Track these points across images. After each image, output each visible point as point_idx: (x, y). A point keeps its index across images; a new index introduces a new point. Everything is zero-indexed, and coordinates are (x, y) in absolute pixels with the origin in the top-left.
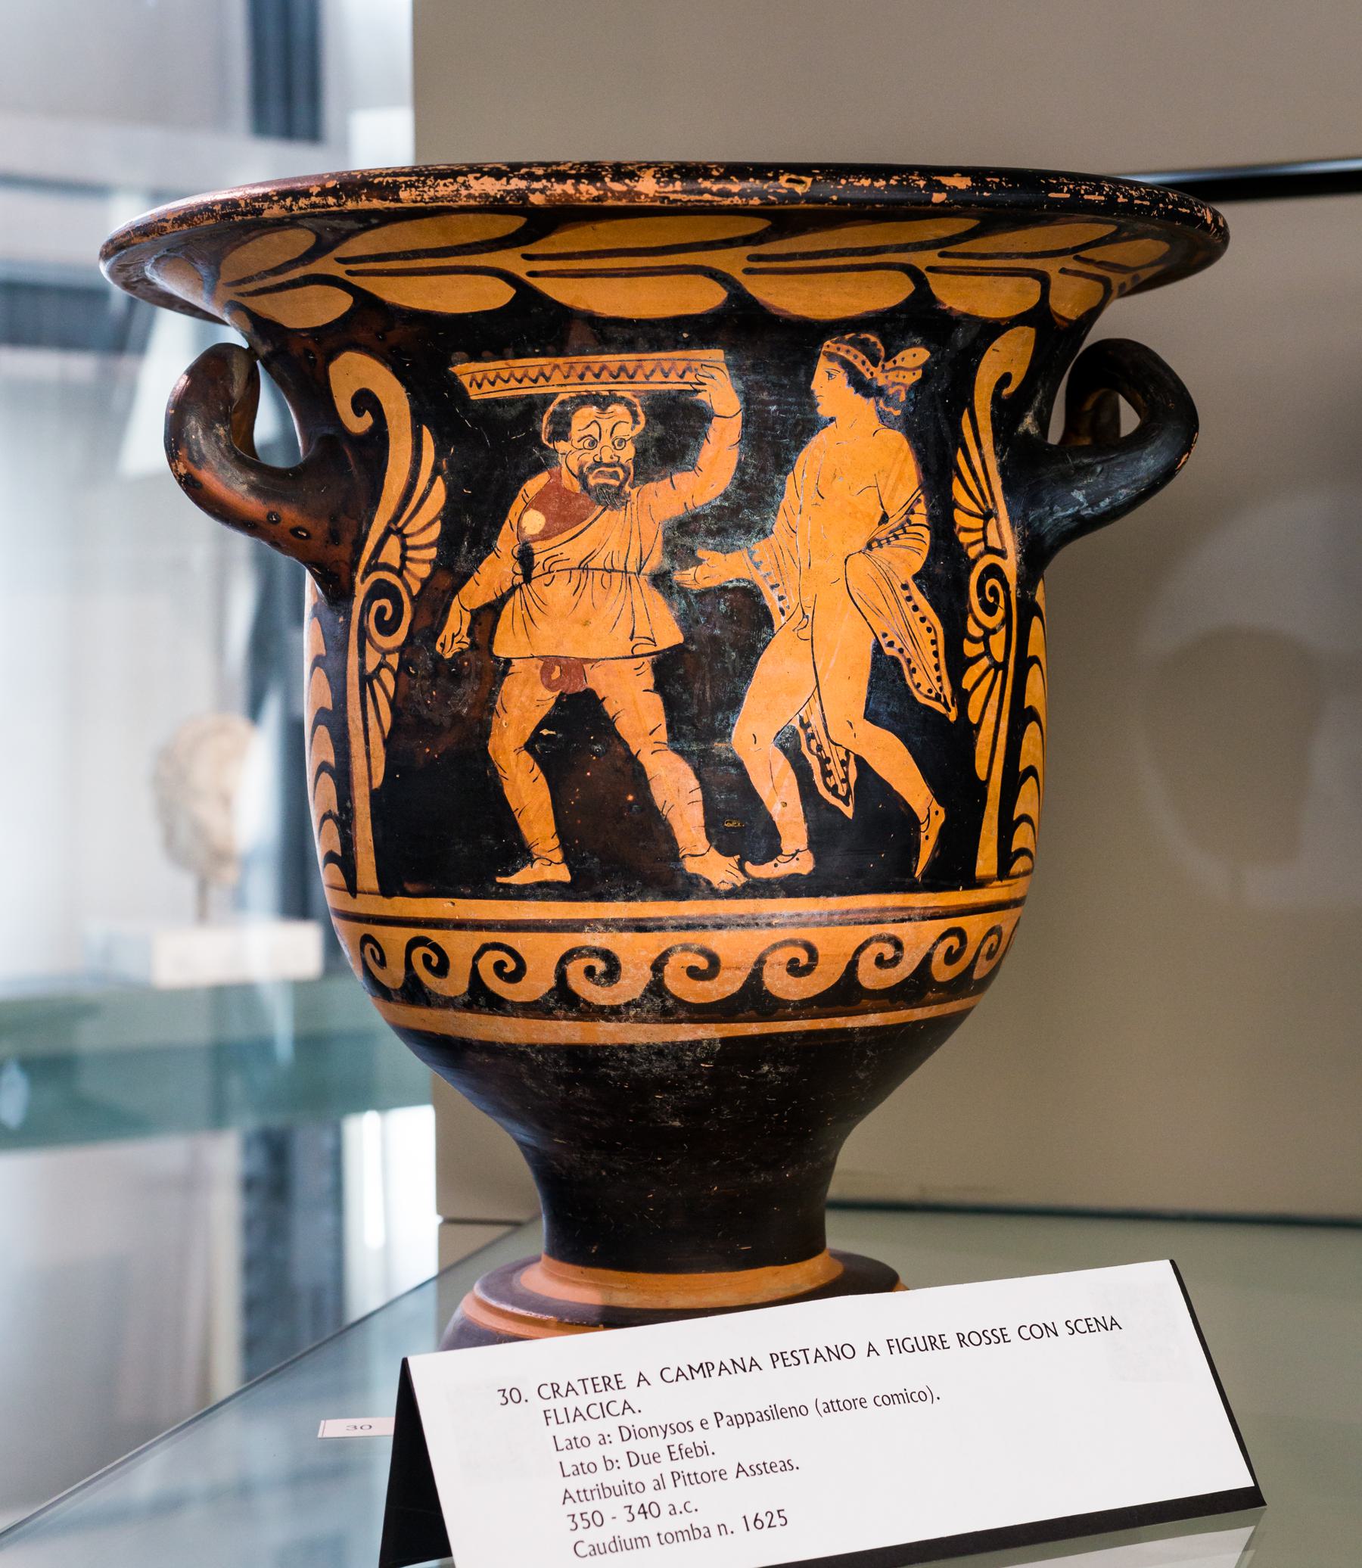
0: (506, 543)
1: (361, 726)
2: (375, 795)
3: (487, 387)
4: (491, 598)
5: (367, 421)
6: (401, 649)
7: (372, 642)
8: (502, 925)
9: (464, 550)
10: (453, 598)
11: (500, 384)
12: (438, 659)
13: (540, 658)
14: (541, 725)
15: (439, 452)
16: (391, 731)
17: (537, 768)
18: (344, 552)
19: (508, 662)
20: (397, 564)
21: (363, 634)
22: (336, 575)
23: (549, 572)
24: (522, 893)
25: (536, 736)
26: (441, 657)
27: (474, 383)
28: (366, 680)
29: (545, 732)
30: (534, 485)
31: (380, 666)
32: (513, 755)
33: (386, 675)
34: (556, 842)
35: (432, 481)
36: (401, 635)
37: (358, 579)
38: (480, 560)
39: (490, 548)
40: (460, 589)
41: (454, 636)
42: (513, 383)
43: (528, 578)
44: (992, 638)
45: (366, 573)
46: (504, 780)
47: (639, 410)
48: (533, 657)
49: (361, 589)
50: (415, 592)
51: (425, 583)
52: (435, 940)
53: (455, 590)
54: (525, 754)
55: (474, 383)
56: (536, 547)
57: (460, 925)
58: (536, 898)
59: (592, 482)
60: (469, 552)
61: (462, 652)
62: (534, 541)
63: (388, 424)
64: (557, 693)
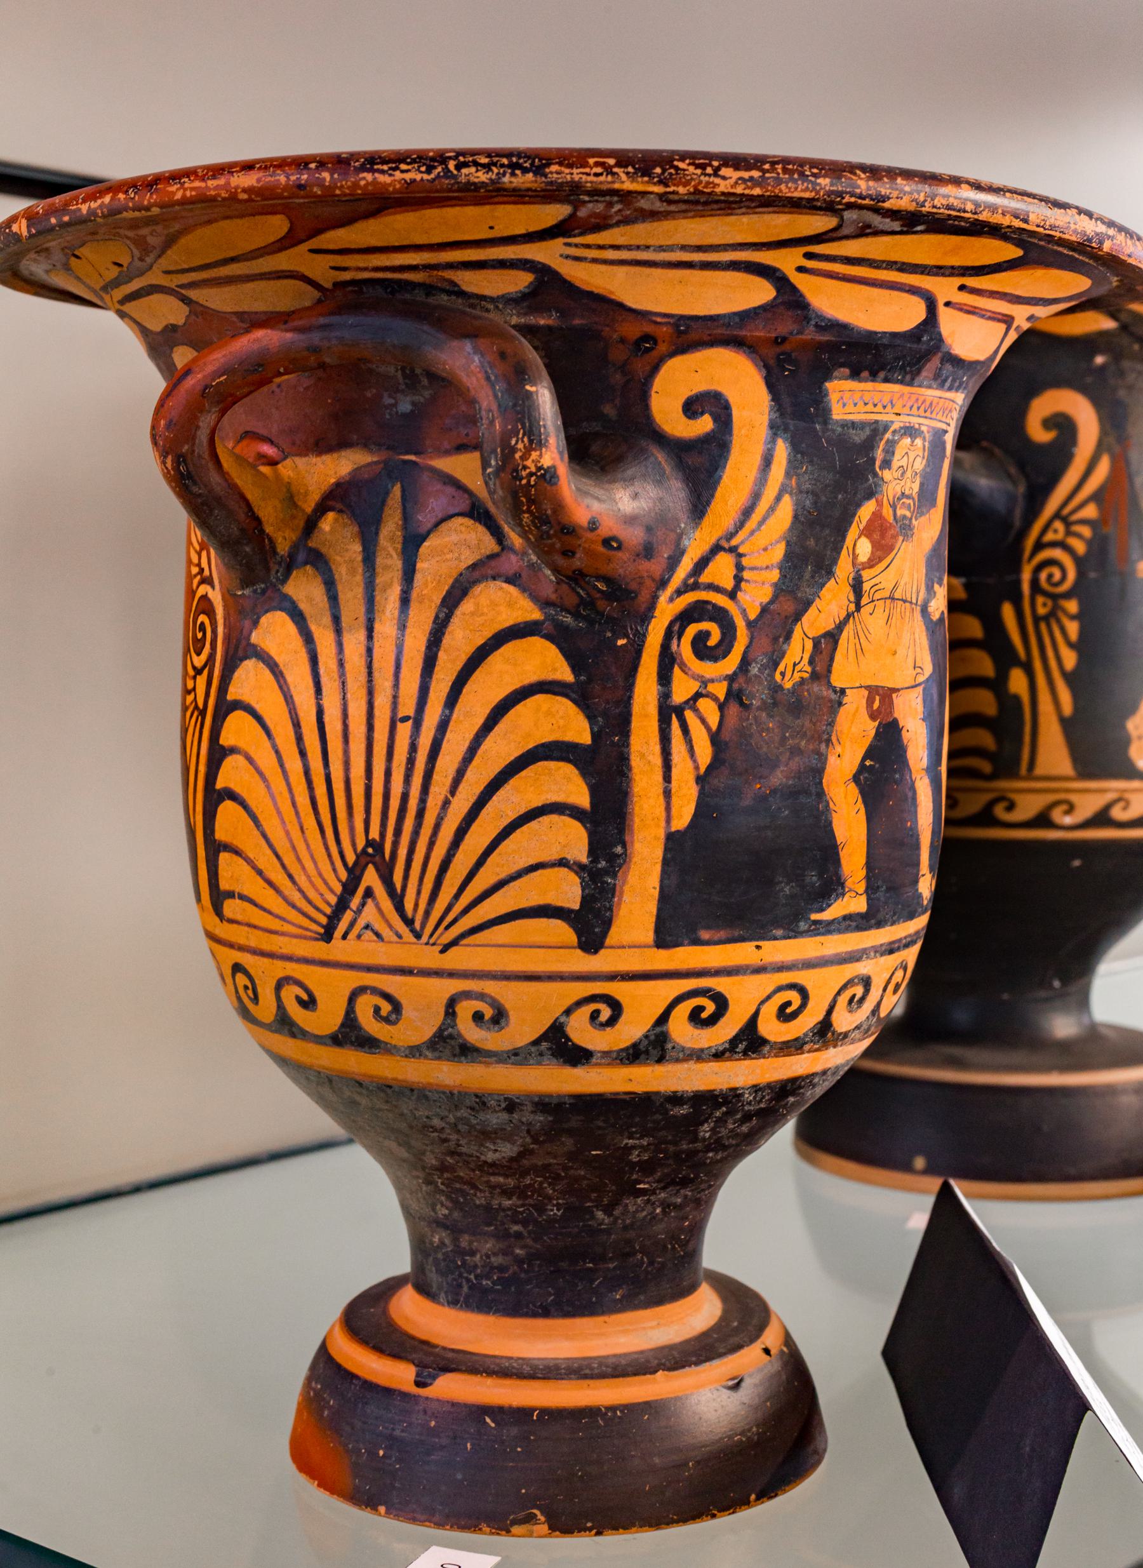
0: (844, 569)
1: (658, 761)
2: (672, 839)
3: (850, 408)
4: (831, 626)
5: (705, 424)
6: (731, 679)
7: (684, 668)
8: (803, 964)
9: (807, 576)
10: (796, 625)
11: (861, 407)
12: (777, 688)
13: (868, 688)
14: (864, 759)
15: (792, 468)
16: (710, 768)
17: (860, 800)
18: (656, 567)
19: (843, 691)
20: (729, 584)
21: (667, 662)
22: (633, 592)
23: (873, 601)
24: (828, 928)
25: (862, 768)
26: (781, 687)
27: (841, 403)
28: (668, 712)
29: (868, 763)
30: (866, 511)
31: (698, 696)
32: (843, 787)
33: (708, 707)
34: (864, 873)
35: (778, 499)
36: (730, 664)
37: (663, 598)
38: (823, 585)
39: (830, 573)
40: (803, 615)
41: (795, 665)
42: (870, 408)
43: (858, 607)
45: (679, 592)
46: (834, 814)
47: (927, 444)
48: (861, 687)
49: (666, 610)
50: (752, 616)
51: (765, 610)
52: (719, 989)
53: (797, 617)
54: (853, 785)
55: (841, 403)
56: (866, 574)
57: (759, 970)
58: (840, 932)
59: (899, 512)
60: (813, 577)
61: (803, 681)
62: (864, 569)
63: (735, 431)
64: (877, 723)
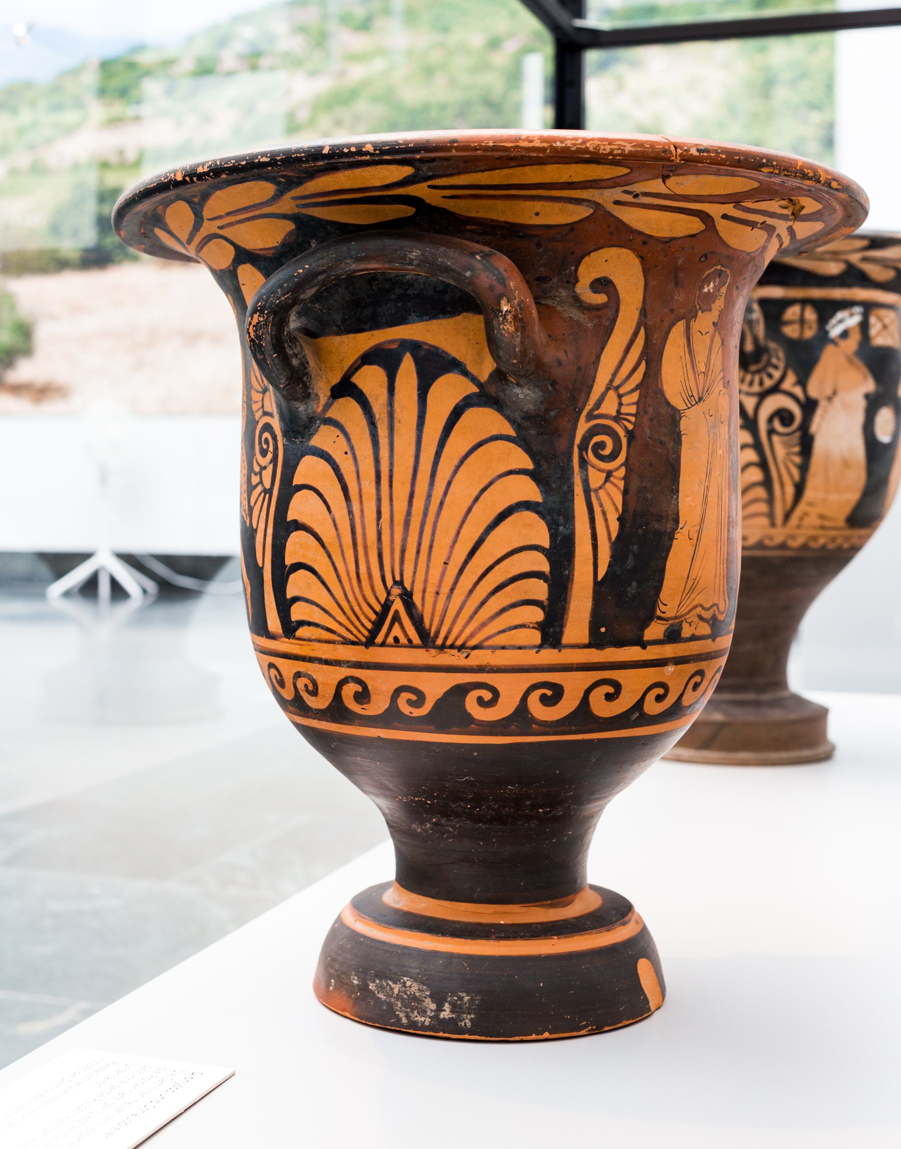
44: (264, 472)
